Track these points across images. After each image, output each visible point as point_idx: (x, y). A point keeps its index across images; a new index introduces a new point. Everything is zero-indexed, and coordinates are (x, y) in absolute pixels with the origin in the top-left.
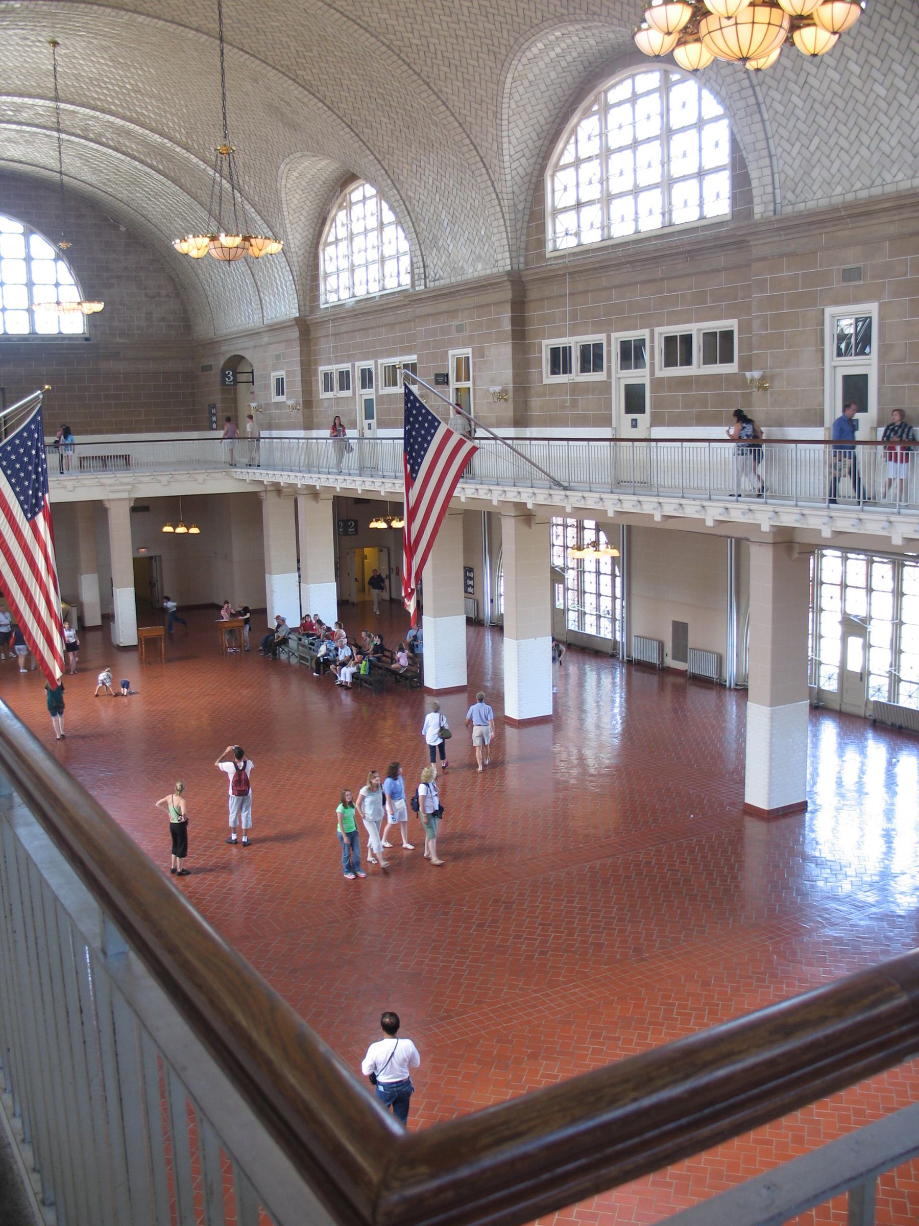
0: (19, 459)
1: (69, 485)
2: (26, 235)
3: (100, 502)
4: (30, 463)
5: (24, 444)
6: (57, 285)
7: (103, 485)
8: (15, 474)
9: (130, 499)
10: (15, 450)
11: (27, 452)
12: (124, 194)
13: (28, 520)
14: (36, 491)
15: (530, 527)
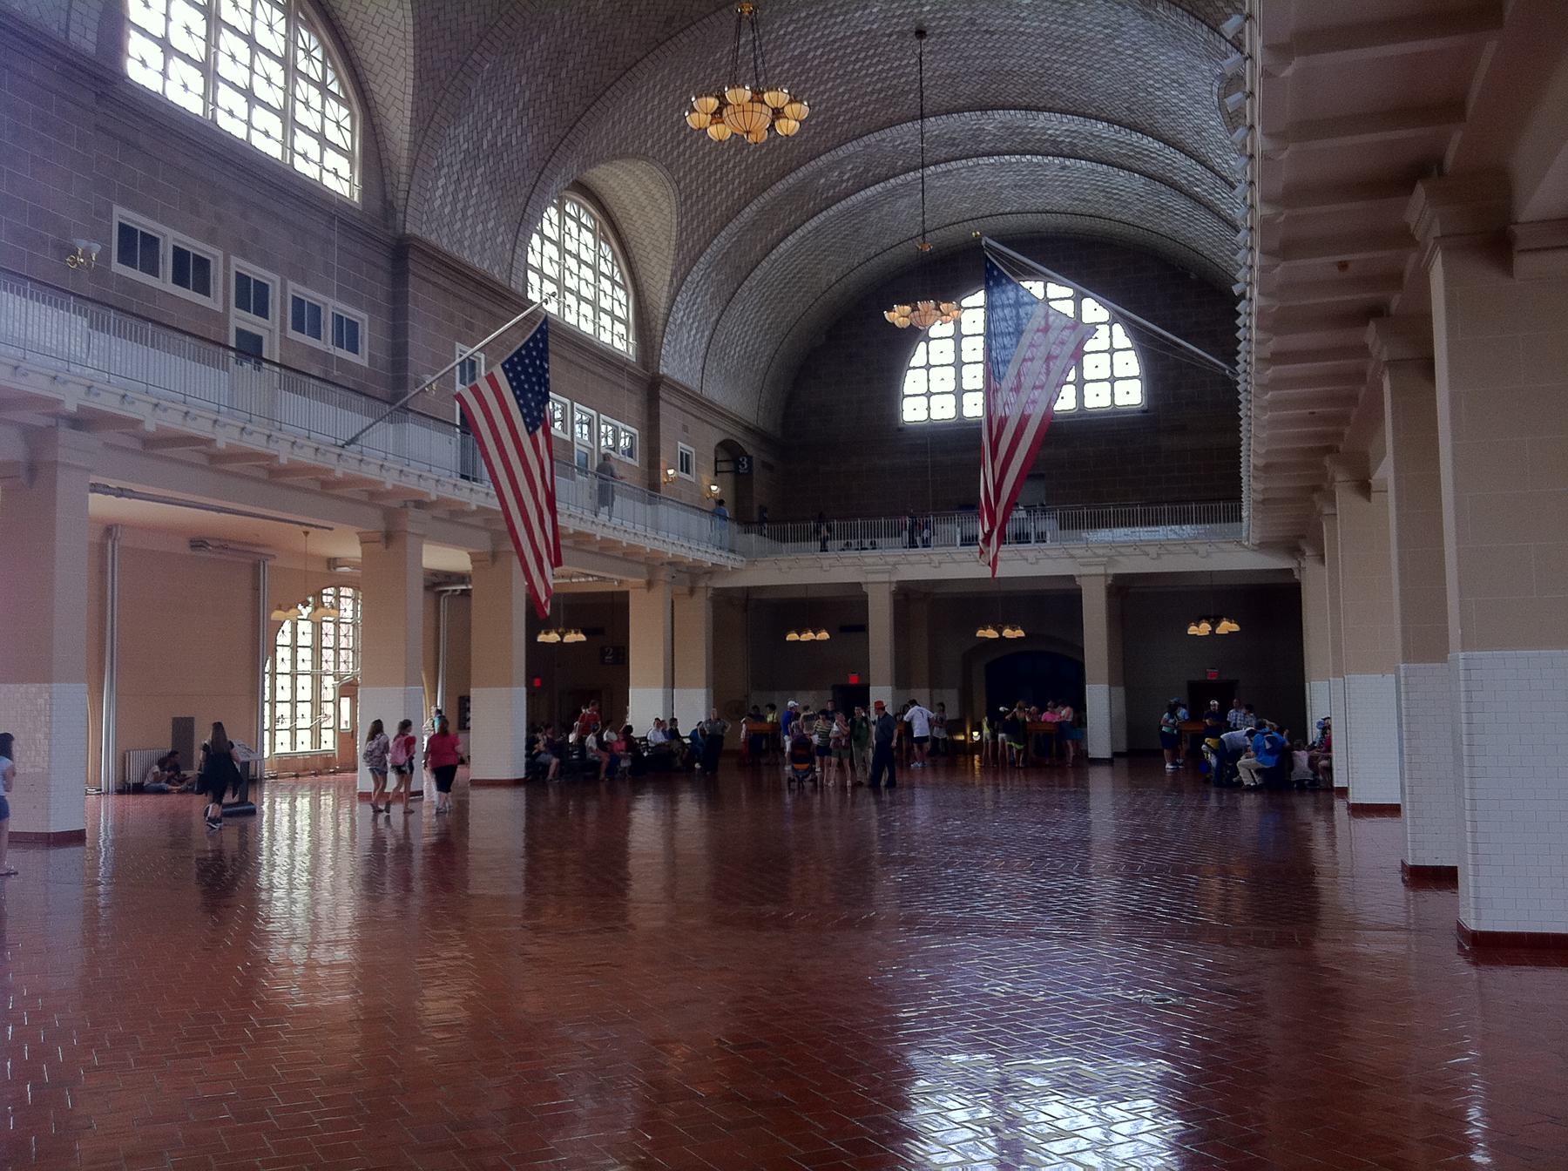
0: (525, 371)
1: (1031, 556)
2: (1078, 300)
3: (1071, 578)
4: (534, 374)
5: (529, 355)
6: (1112, 351)
7: (1072, 557)
8: (521, 384)
9: (1106, 575)
10: (521, 362)
11: (533, 363)
12: (1165, 228)
13: (530, 433)
14: (537, 405)
15: (1369, 500)
